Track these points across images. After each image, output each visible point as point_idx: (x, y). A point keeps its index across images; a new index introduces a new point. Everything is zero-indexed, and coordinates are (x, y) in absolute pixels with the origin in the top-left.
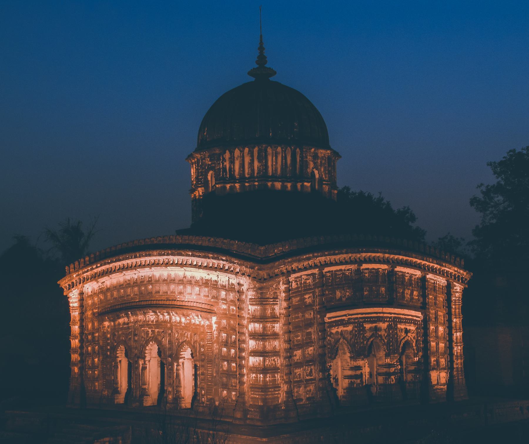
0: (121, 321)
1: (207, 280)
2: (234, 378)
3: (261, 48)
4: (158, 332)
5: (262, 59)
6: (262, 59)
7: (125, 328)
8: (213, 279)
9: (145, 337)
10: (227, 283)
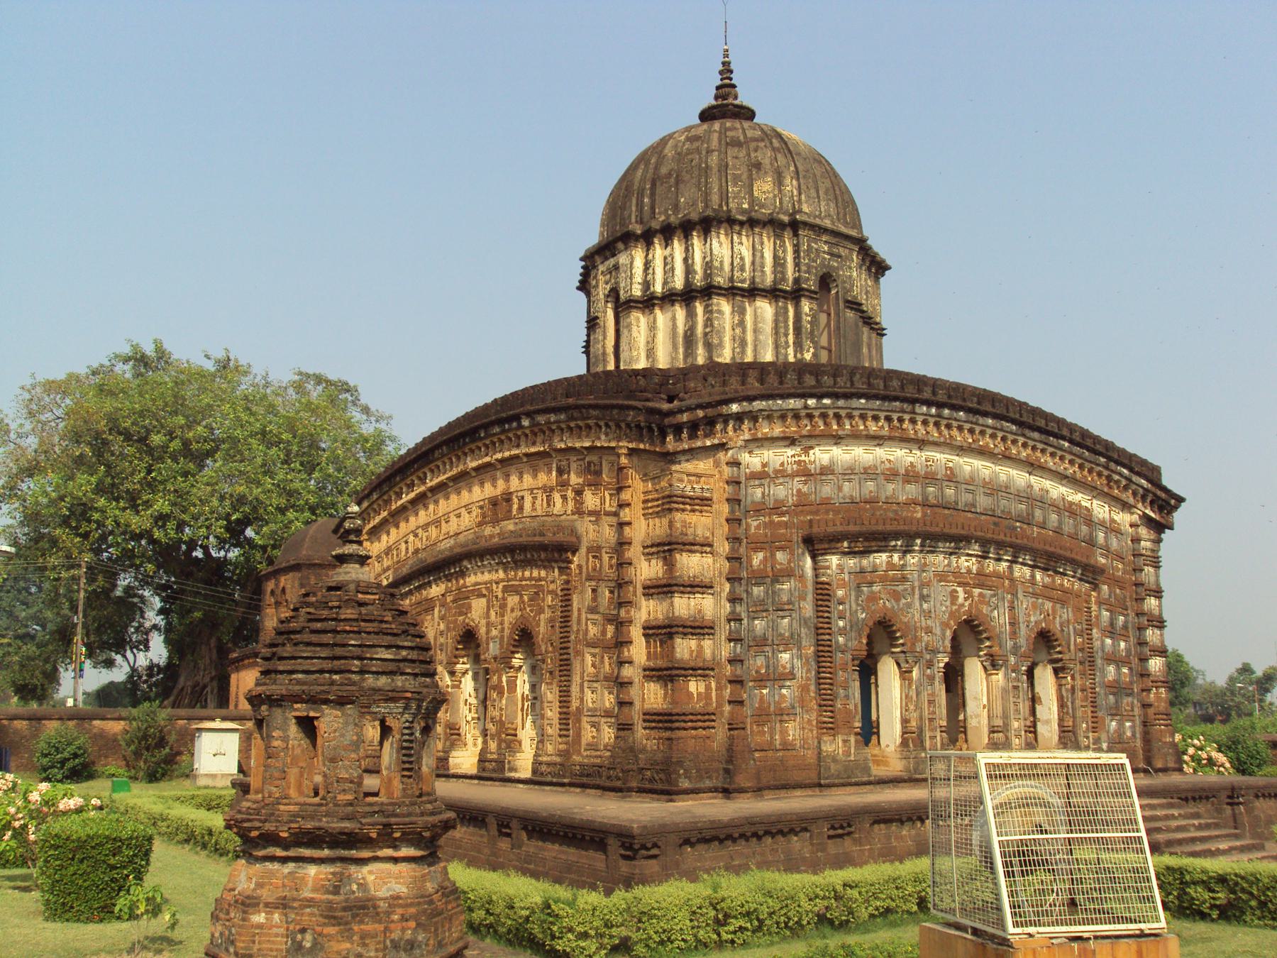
0: (881, 558)
1: (1071, 504)
2: (1128, 695)
3: (726, 70)
4: (980, 595)
5: (726, 88)
6: (726, 88)
7: (894, 579)
8: (1084, 504)
9: (948, 603)
10: (1107, 516)
